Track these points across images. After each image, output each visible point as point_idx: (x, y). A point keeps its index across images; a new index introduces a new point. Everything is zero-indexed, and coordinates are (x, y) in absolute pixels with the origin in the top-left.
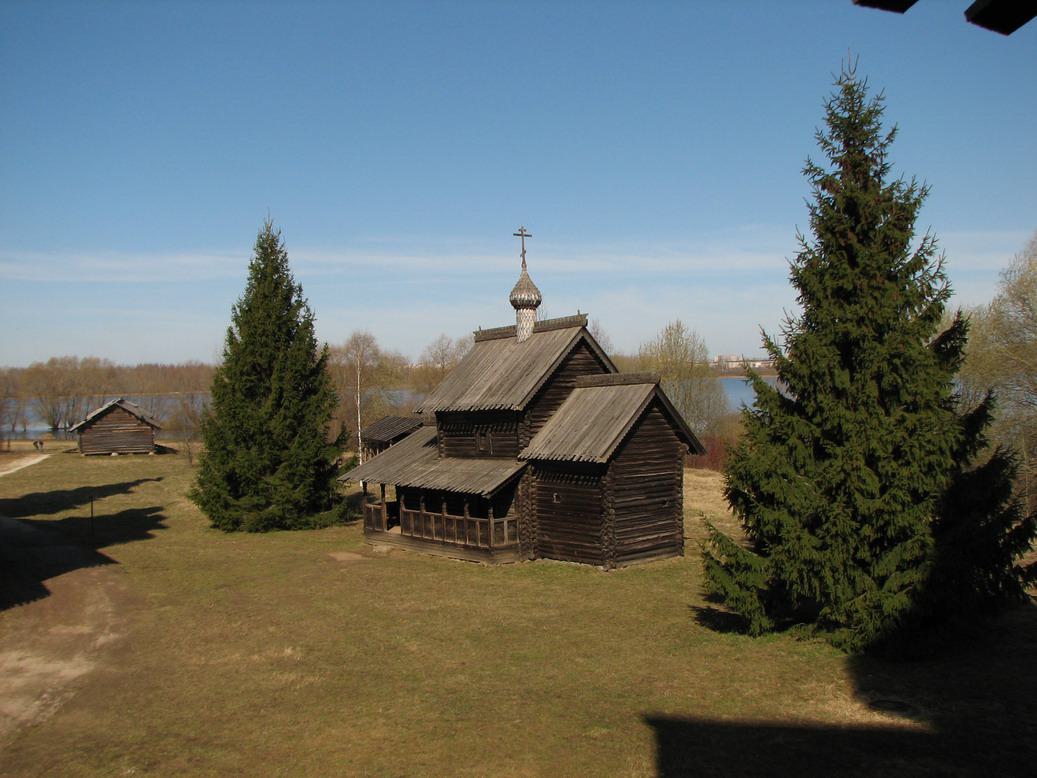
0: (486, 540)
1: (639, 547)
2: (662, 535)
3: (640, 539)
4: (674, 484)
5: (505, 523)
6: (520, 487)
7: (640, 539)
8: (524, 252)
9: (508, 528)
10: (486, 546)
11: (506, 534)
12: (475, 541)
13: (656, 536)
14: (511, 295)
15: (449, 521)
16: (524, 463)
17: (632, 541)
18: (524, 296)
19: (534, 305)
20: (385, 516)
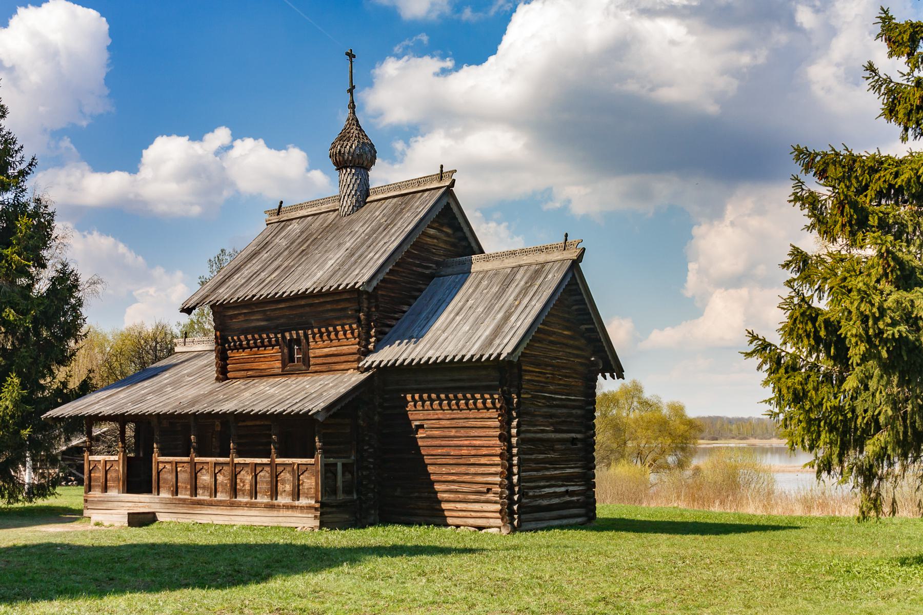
1: (545, 502)
2: (571, 488)
3: (547, 490)
7: (547, 490)
8: (353, 87)
13: (563, 489)
14: (334, 145)
16: (366, 375)
17: (537, 492)
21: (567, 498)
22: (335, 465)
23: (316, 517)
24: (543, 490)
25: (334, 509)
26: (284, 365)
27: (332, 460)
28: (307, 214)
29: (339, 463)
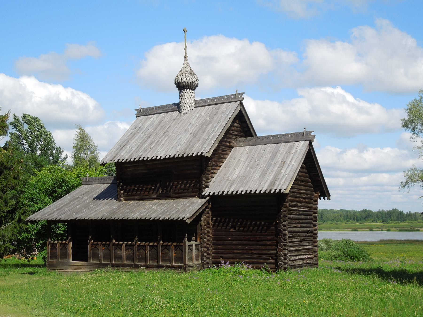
0: (181, 259)
1: (297, 263)
2: (307, 256)
4: (311, 219)
6: (202, 219)
8: (186, 47)
11: (194, 256)
12: (170, 261)
13: (304, 257)
17: (293, 258)
19: (193, 86)
21: (306, 261)
22: (192, 245)
24: (296, 257)
27: (191, 243)
28: (161, 112)
29: (193, 245)
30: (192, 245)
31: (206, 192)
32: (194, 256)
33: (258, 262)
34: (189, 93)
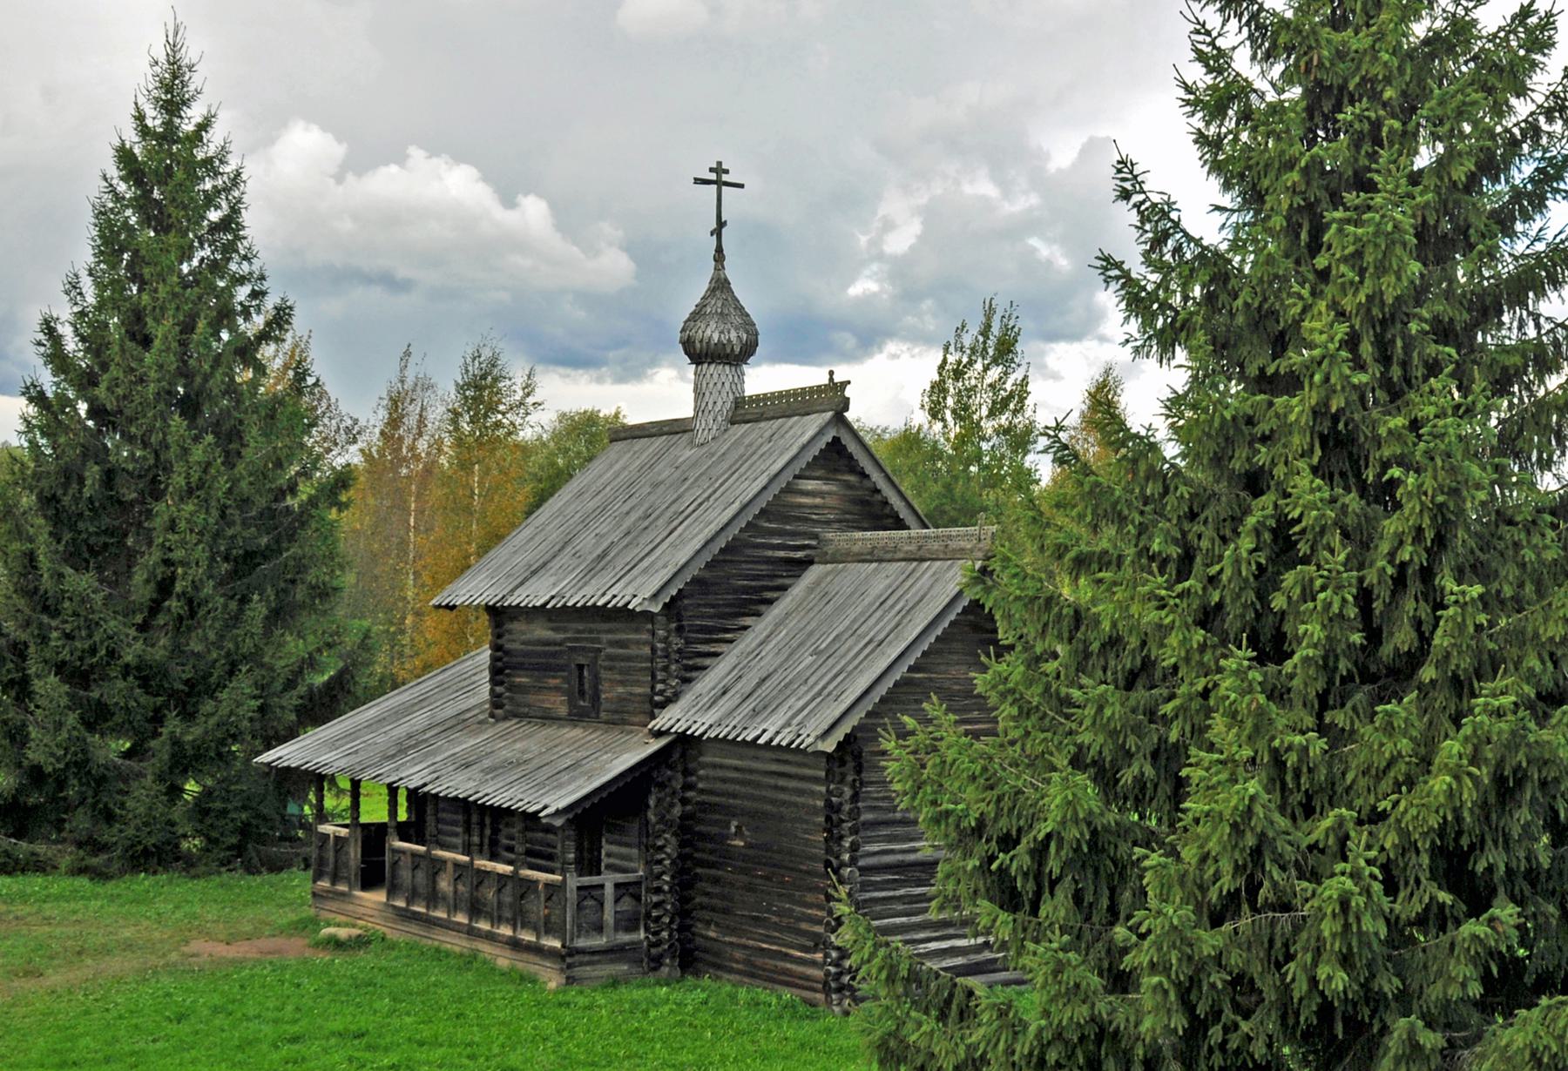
3: (933, 946)
5: (609, 890)
6: (652, 803)
7: (933, 946)
8: (721, 224)
9: (617, 901)
10: (557, 944)
11: (609, 916)
14: (683, 330)
15: (484, 875)
16: (663, 742)
18: (712, 332)
20: (354, 853)
22: (602, 886)
23: (562, 970)
25: (596, 958)
26: (571, 703)
30: (602, 886)
31: (663, 720)
32: (609, 916)
33: (786, 955)
34: (715, 376)
